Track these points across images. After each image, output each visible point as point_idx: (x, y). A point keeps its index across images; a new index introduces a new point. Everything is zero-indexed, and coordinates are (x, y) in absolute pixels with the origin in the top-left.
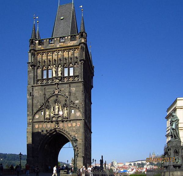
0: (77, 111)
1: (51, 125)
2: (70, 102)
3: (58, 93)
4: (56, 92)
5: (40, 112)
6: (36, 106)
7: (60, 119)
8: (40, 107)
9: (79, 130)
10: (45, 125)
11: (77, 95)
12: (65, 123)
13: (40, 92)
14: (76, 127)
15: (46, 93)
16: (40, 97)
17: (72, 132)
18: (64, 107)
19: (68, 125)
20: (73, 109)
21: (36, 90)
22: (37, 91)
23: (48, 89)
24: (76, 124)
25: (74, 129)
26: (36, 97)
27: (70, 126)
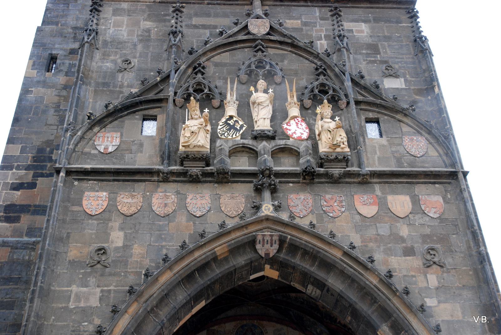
0: (405, 129)
1: (217, 198)
2: (352, 80)
3: (268, 34)
4: (259, 27)
5: (138, 116)
6: (105, 84)
7: (287, 165)
8: (134, 91)
9: (443, 239)
10: (163, 199)
11: (386, 52)
12: (333, 200)
13: (148, 24)
14: (418, 219)
15: (185, 30)
16: (140, 47)
17: (389, 252)
18: (316, 101)
19: (351, 207)
20: (371, 115)
21: (114, 14)
22: (125, 19)
23: (196, 15)
24: (415, 201)
25: (404, 231)
26: (118, 44)
27: (369, 211)
